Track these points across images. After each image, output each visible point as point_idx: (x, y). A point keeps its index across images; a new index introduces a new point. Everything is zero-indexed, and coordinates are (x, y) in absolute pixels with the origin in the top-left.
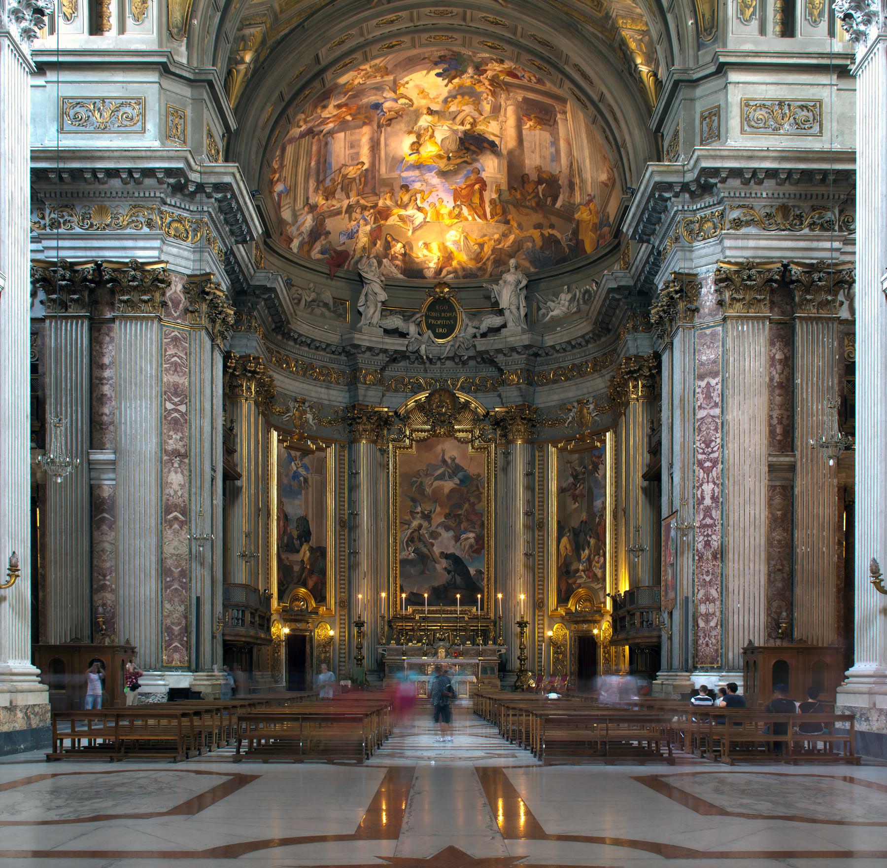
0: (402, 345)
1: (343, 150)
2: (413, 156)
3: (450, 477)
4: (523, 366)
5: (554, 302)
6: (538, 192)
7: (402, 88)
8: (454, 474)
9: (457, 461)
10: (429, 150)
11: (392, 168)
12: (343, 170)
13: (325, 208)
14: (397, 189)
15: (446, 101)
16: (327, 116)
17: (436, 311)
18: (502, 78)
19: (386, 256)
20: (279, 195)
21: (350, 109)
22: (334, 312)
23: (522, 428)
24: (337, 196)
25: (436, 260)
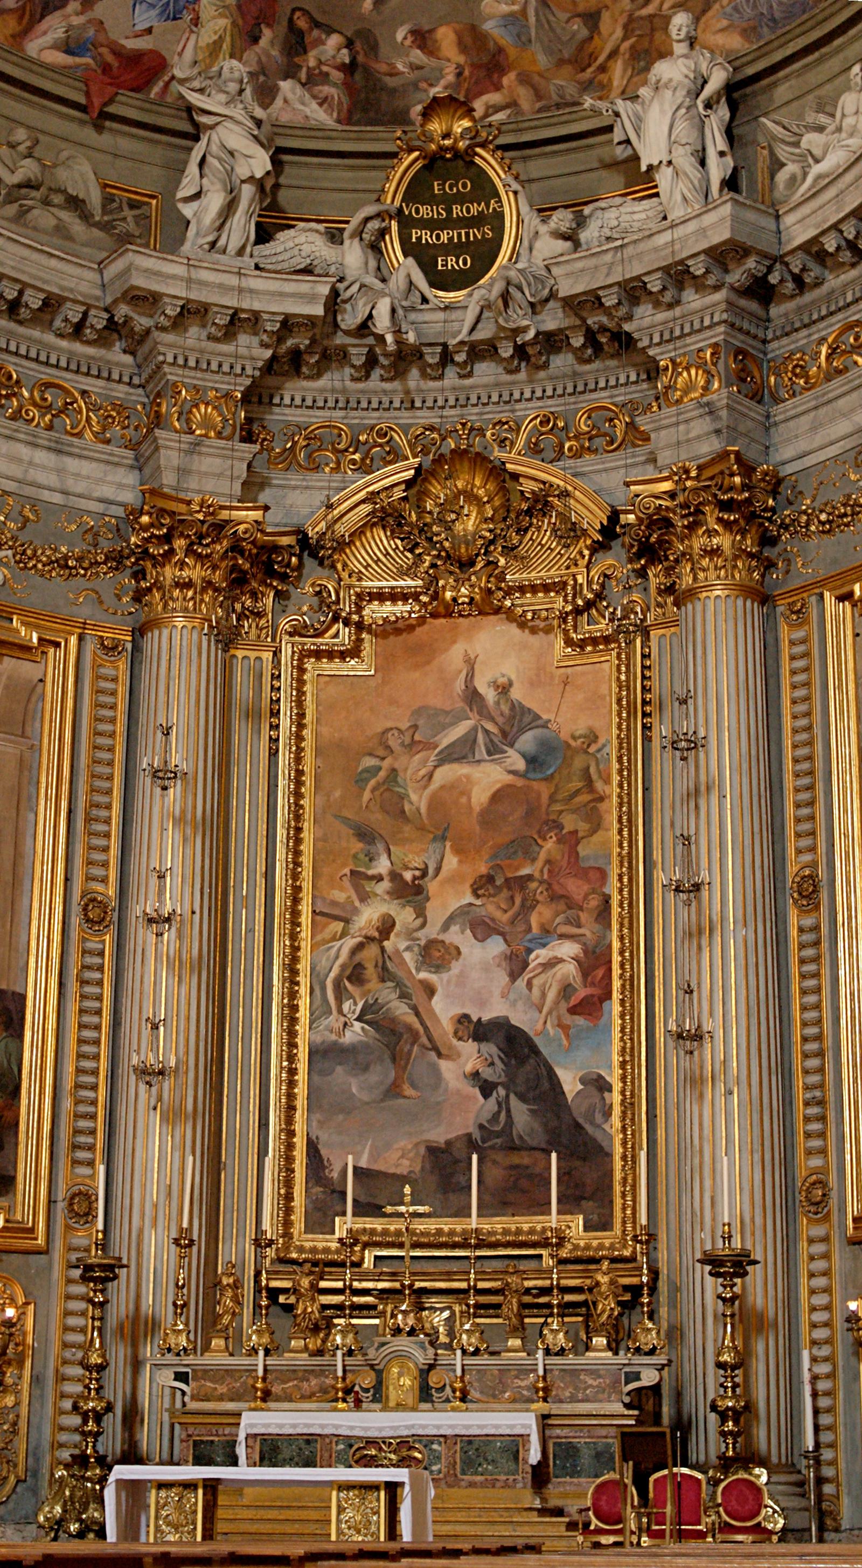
0: (311, 298)
3: (493, 750)
4: (719, 334)
5: (821, 129)
8: (508, 736)
9: (516, 694)
17: (432, 200)
19: (290, 73)
22: (105, 227)
23: (724, 541)
25: (451, 78)
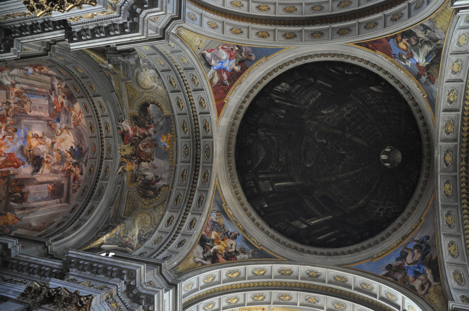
1: (39, 103)
2: (31, 135)
6: (16, 193)
7: (66, 131)
10: (34, 142)
11: (26, 125)
12: (29, 102)
13: (12, 91)
14: (15, 127)
15: (58, 150)
16: (59, 98)
18: (72, 174)
20: (27, 70)
21: (59, 108)
24: (16, 98)
